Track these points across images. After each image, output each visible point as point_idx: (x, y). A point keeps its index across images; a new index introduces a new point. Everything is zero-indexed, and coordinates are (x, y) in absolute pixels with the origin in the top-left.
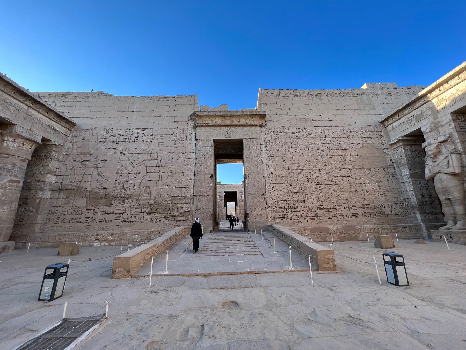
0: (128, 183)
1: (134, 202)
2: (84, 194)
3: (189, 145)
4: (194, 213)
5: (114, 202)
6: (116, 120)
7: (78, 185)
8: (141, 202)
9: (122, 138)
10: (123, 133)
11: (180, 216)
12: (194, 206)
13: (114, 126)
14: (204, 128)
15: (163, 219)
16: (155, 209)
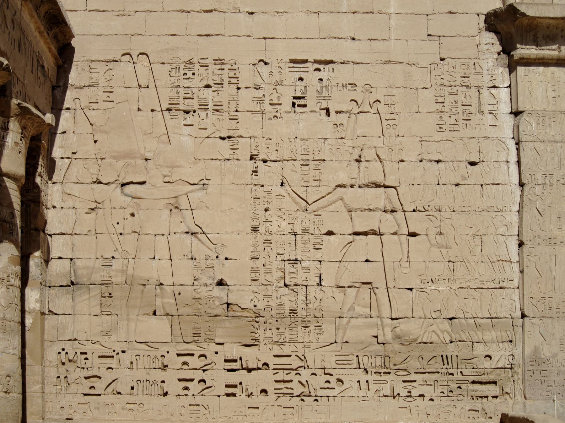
0: (298, 266)
1: (329, 332)
2: (159, 301)
3: (492, 133)
4: (528, 374)
5: (261, 332)
6: (211, 23)
7: (130, 272)
8: (350, 335)
9: (246, 99)
10: (246, 76)
11: (481, 383)
12: (528, 351)
13: (210, 50)
14: (541, 69)
15: (428, 391)
16: (399, 359)
